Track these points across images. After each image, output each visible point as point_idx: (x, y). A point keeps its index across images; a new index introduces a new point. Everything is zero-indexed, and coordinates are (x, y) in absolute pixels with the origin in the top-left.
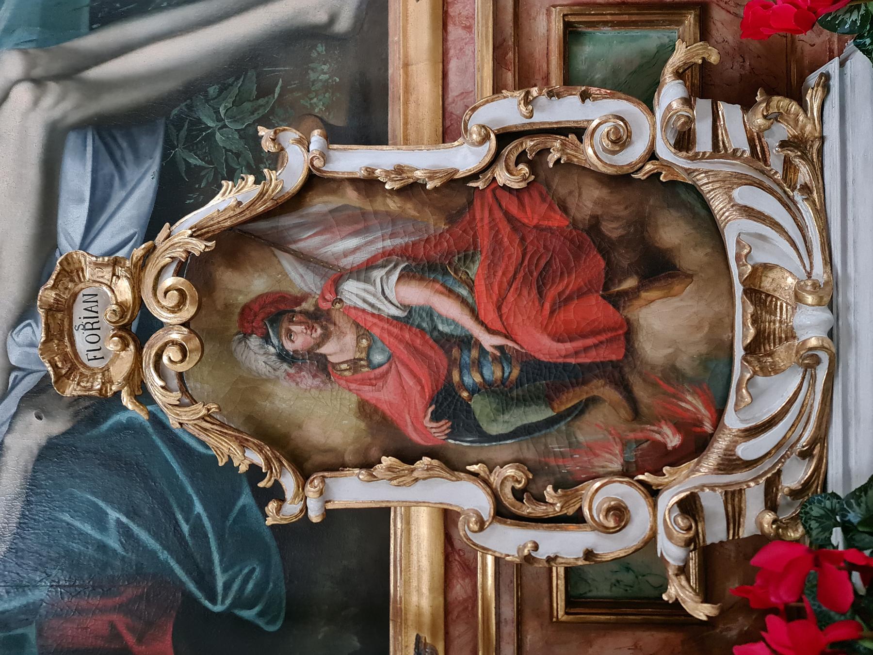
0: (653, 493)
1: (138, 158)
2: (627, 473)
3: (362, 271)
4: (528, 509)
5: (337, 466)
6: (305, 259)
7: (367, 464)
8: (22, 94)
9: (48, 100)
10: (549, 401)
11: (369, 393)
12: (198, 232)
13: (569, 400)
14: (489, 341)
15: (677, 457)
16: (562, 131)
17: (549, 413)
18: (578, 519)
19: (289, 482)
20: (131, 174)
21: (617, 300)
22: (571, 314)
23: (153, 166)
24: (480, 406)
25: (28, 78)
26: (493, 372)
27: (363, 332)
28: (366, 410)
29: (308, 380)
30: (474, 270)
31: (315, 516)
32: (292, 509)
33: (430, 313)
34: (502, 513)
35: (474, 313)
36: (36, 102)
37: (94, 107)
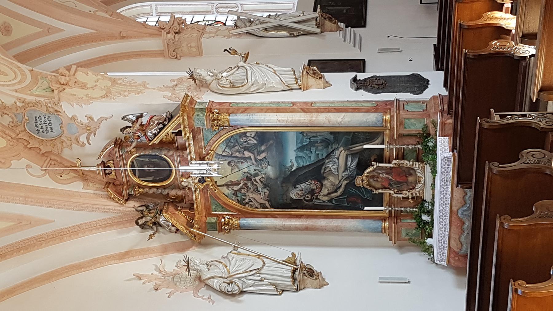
0: (409, 192)
1: (356, 157)
2: (407, 190)
3: (382, 174)
4: (398, 193)
5: (379, 189)
6: (376, 172)
7: (382, 189)
8: (343, 151)
9: (346, 152)
10: (400, 184)
11: (382, 183)
12: (367, 173)
13: (401, 185)
14: (394, 180)
15: (412, 189)
16: (402, 163)
17: (399, 185)
18: (402, 194)
19: (375, 191)
20: (355, 159)
21: (406, 177)
22: (401, 178)
23: (358, 158)
24: (393, 185)
25: (344, 150)
26: (394, 182)
27: (381, 178)
28: (382, 184)
29: (376, 182)
30: (393, 174)
31: (377, 193)
32: (375, 192)
33: (388, 177)
34: (395, 193)
35: (393, 178)
36: (345, 152)
37: (351, 153)
